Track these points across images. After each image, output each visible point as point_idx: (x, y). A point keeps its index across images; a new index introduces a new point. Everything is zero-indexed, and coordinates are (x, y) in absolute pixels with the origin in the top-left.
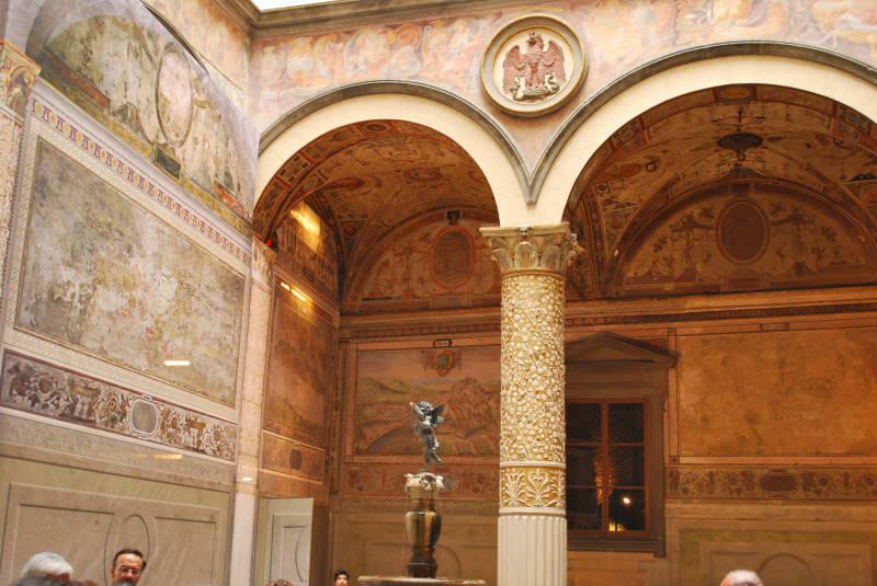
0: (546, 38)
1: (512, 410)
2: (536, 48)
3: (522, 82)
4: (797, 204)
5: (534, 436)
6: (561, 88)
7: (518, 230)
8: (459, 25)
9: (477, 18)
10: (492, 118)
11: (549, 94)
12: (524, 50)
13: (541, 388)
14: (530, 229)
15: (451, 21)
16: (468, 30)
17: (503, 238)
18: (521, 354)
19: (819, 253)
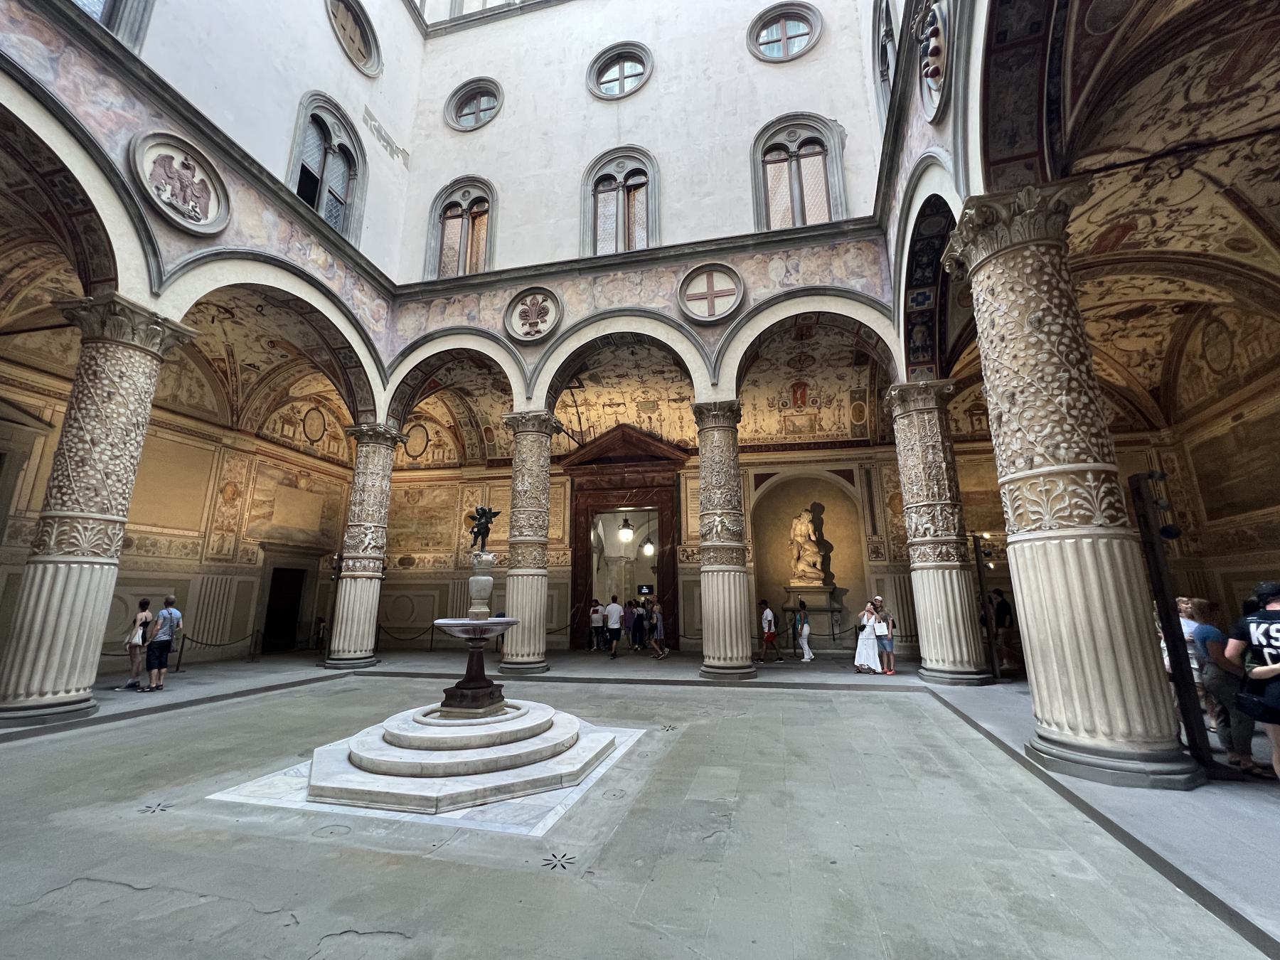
0: (199, 175)
1: (100, 466)
2: (187, 173)
3: (169, 188)
4: (184, 355)
5: (120, 494)
6: (202, 222)
7: (154, 315)
8: (112, 83)
9: (136, 96)
10: (137, 198)
11: (191, 218)
12: (176, 164)
13: (135, 454)
14: (166, 320)
15: (102, 70)
16: (123, 98)
17: (132, 312)
18: (123, 419)
19: (189, 391)
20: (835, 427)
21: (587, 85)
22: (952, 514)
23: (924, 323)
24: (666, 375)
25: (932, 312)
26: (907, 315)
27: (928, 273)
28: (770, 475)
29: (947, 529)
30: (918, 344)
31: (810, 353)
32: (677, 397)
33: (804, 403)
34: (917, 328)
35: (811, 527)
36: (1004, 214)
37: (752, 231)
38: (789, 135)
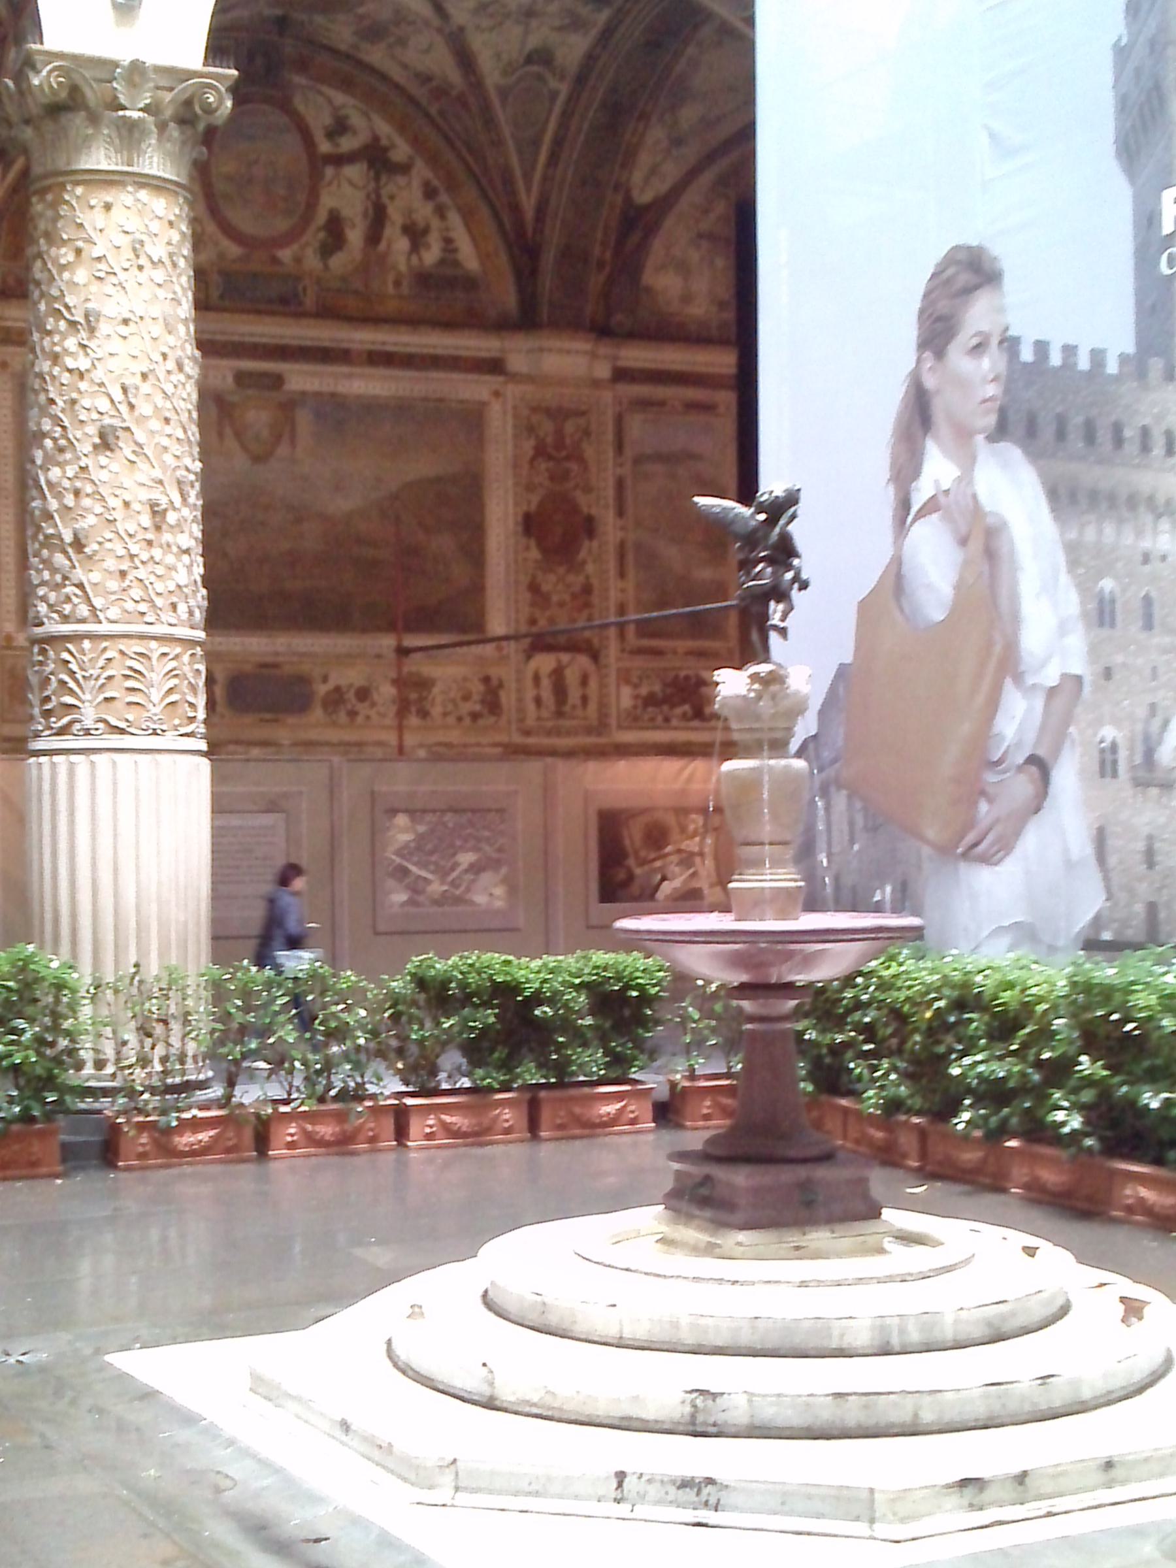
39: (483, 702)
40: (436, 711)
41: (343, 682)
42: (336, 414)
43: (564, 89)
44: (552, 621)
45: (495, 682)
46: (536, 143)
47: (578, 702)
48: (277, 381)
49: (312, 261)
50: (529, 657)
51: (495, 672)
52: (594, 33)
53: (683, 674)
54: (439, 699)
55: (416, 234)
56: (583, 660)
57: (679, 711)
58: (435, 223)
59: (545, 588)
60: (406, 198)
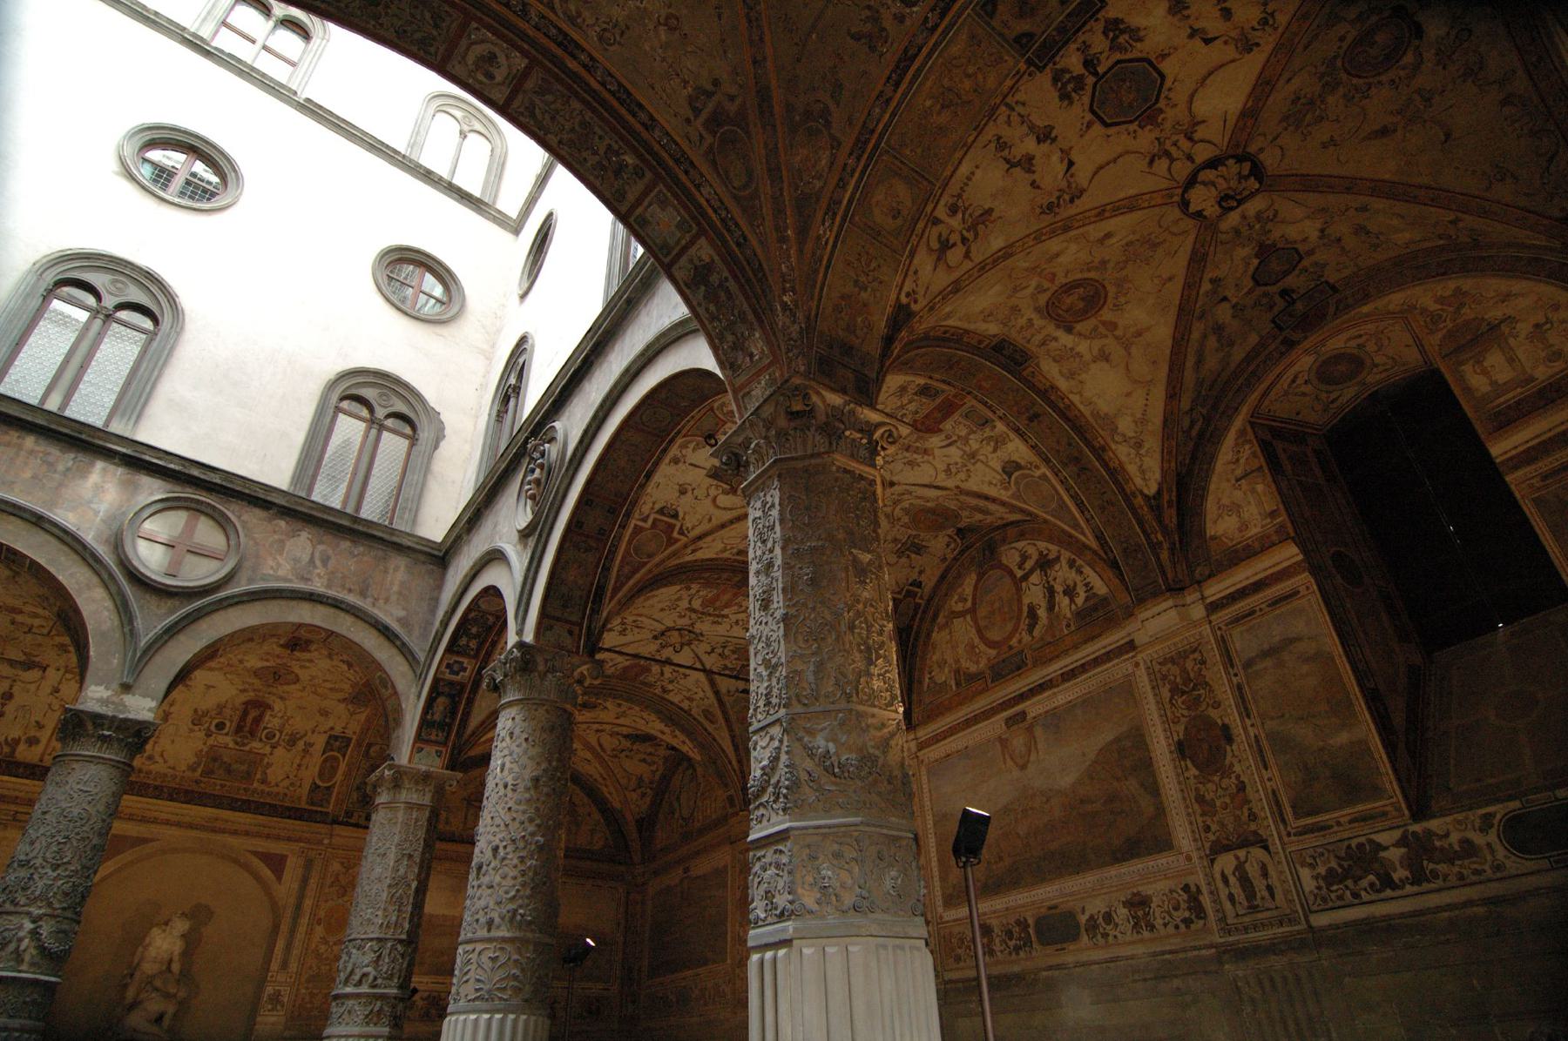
20: (286, 783)
21: (120, 148)
22: (403, 956)
23: (452, 697)
24: (19, 618)
25: (462, 686)
26: (436, 681)
27: (473, 644)
28: (145, 841)
29: (390, 978)
30: (437, 717)
31: (297, 670)
32: (23, 658)
33: (252, 733)
34: (441, 700)
35: (178, 946)
36: (541, 668)
37: (284, 488)
38: (381, 395)
39: (1189, 909)
40: (1158, 922)
41: (1095, 911)
42: (1055, 720)
43: (1044, 470)
44: (1223, 825)
45: (1193, 889)
46: (1063, 505)
47: (1266, 894)
48: (1024, 714)
49: (1026, 638)
50: (1212, 861)
51: (1191, 880)
52: (1012, 435)
53: (1354, 843)
54: (1158, 911)
55: (1070, 592)
56: (1257, 852)
57: (1364, 883)
58: (1079, 579)
59: (1208, 797)
60: (1063, 574)
